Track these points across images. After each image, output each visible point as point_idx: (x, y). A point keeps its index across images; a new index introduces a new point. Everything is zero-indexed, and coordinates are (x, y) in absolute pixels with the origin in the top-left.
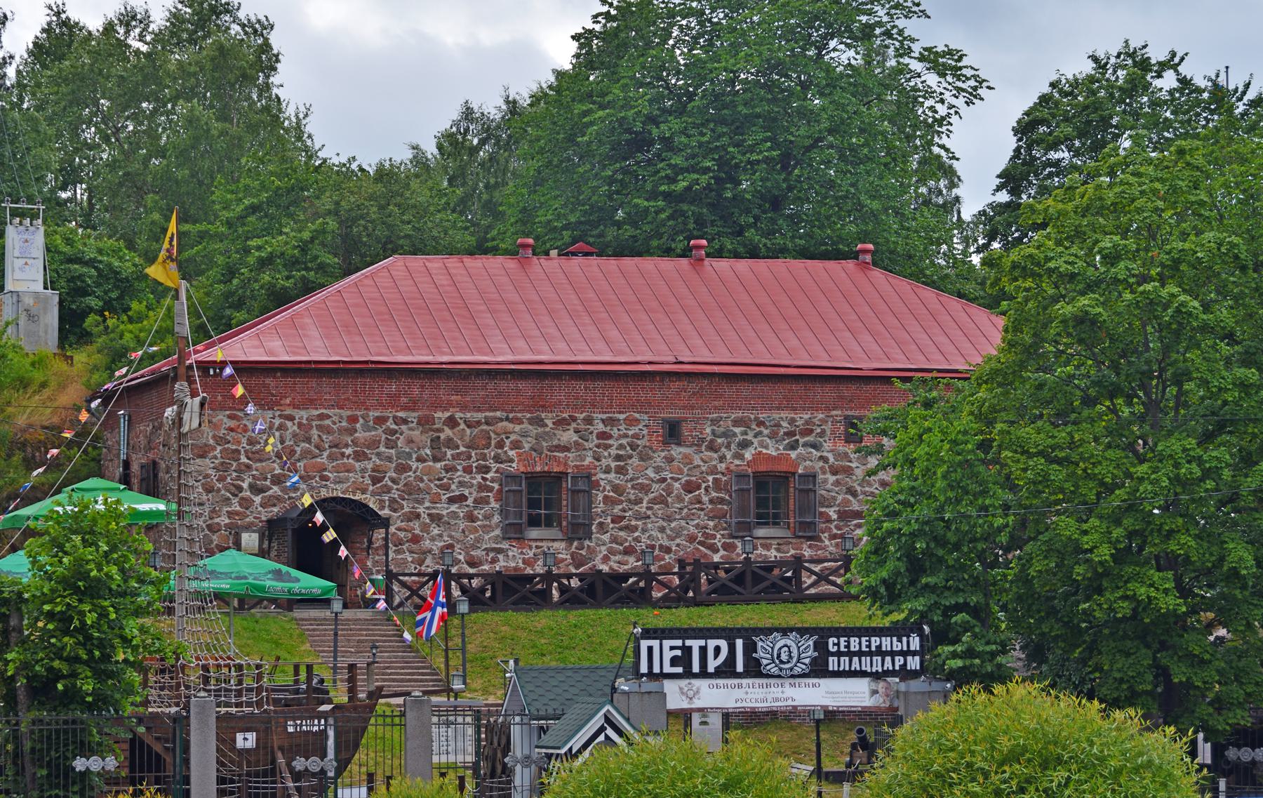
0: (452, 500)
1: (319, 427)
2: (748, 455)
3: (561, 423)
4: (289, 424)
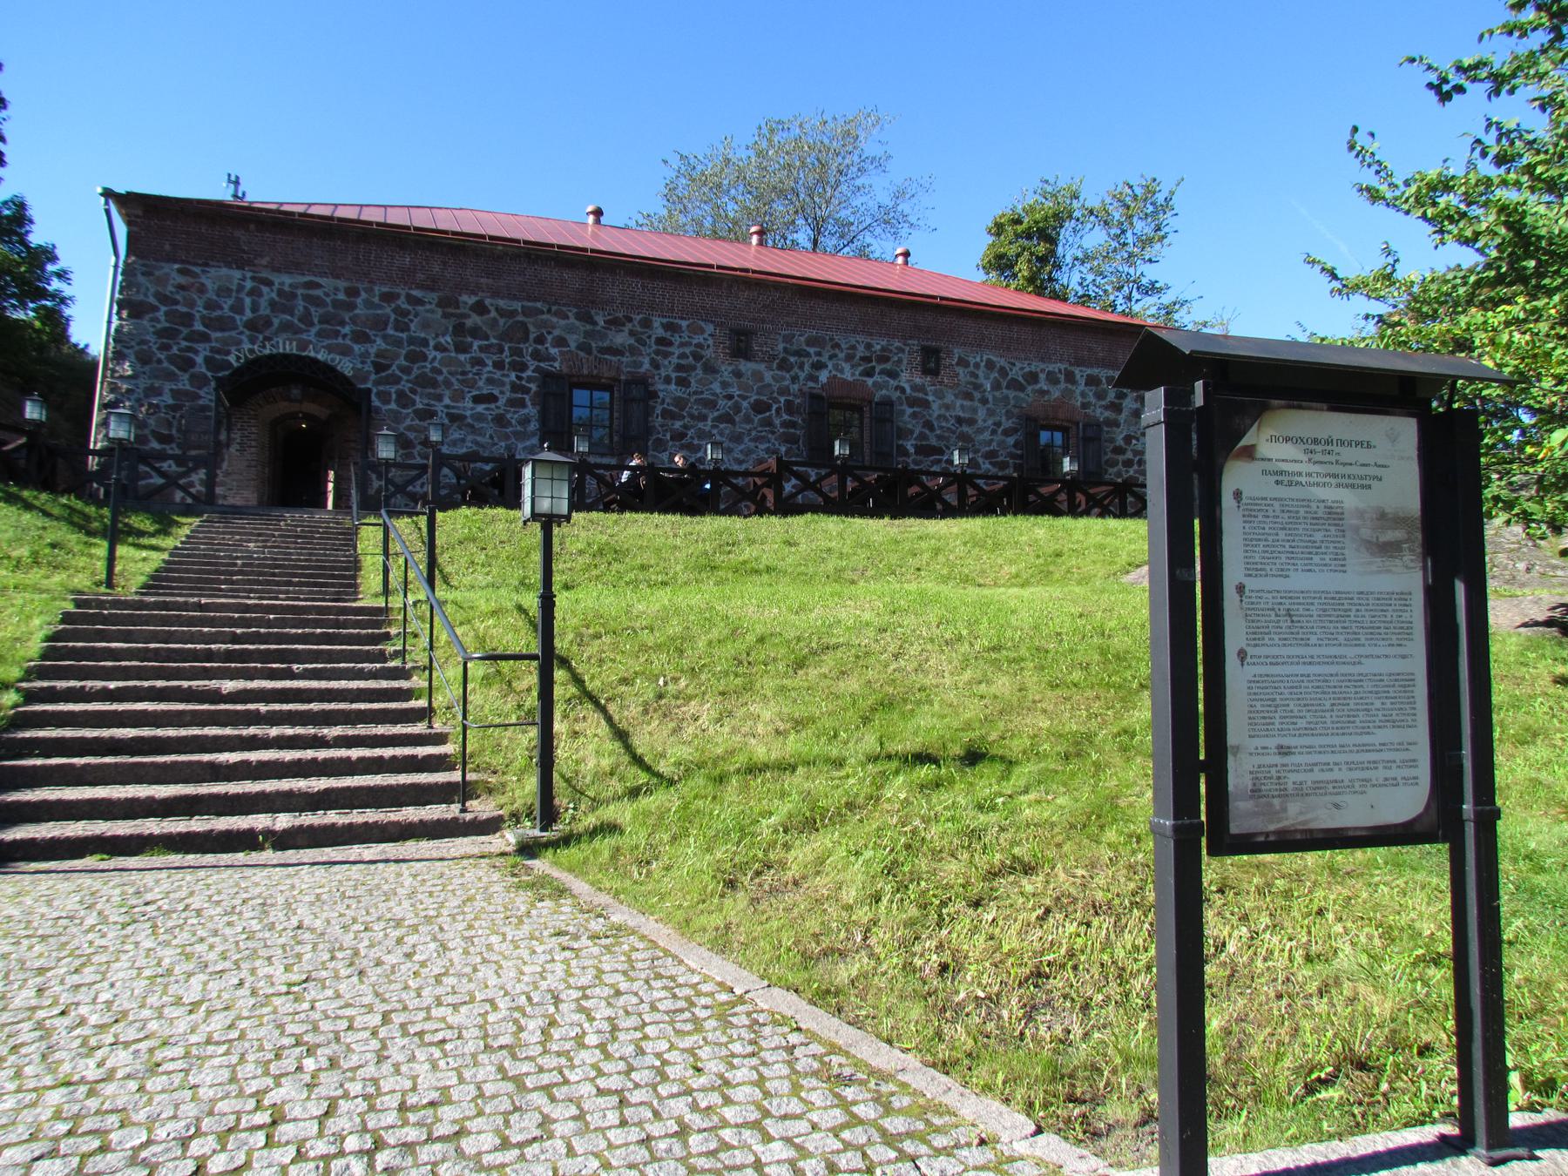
0: (478, 400)
1: (307, 298)
2: (823, 376)
3: (614, 323)
4: (265, 289)
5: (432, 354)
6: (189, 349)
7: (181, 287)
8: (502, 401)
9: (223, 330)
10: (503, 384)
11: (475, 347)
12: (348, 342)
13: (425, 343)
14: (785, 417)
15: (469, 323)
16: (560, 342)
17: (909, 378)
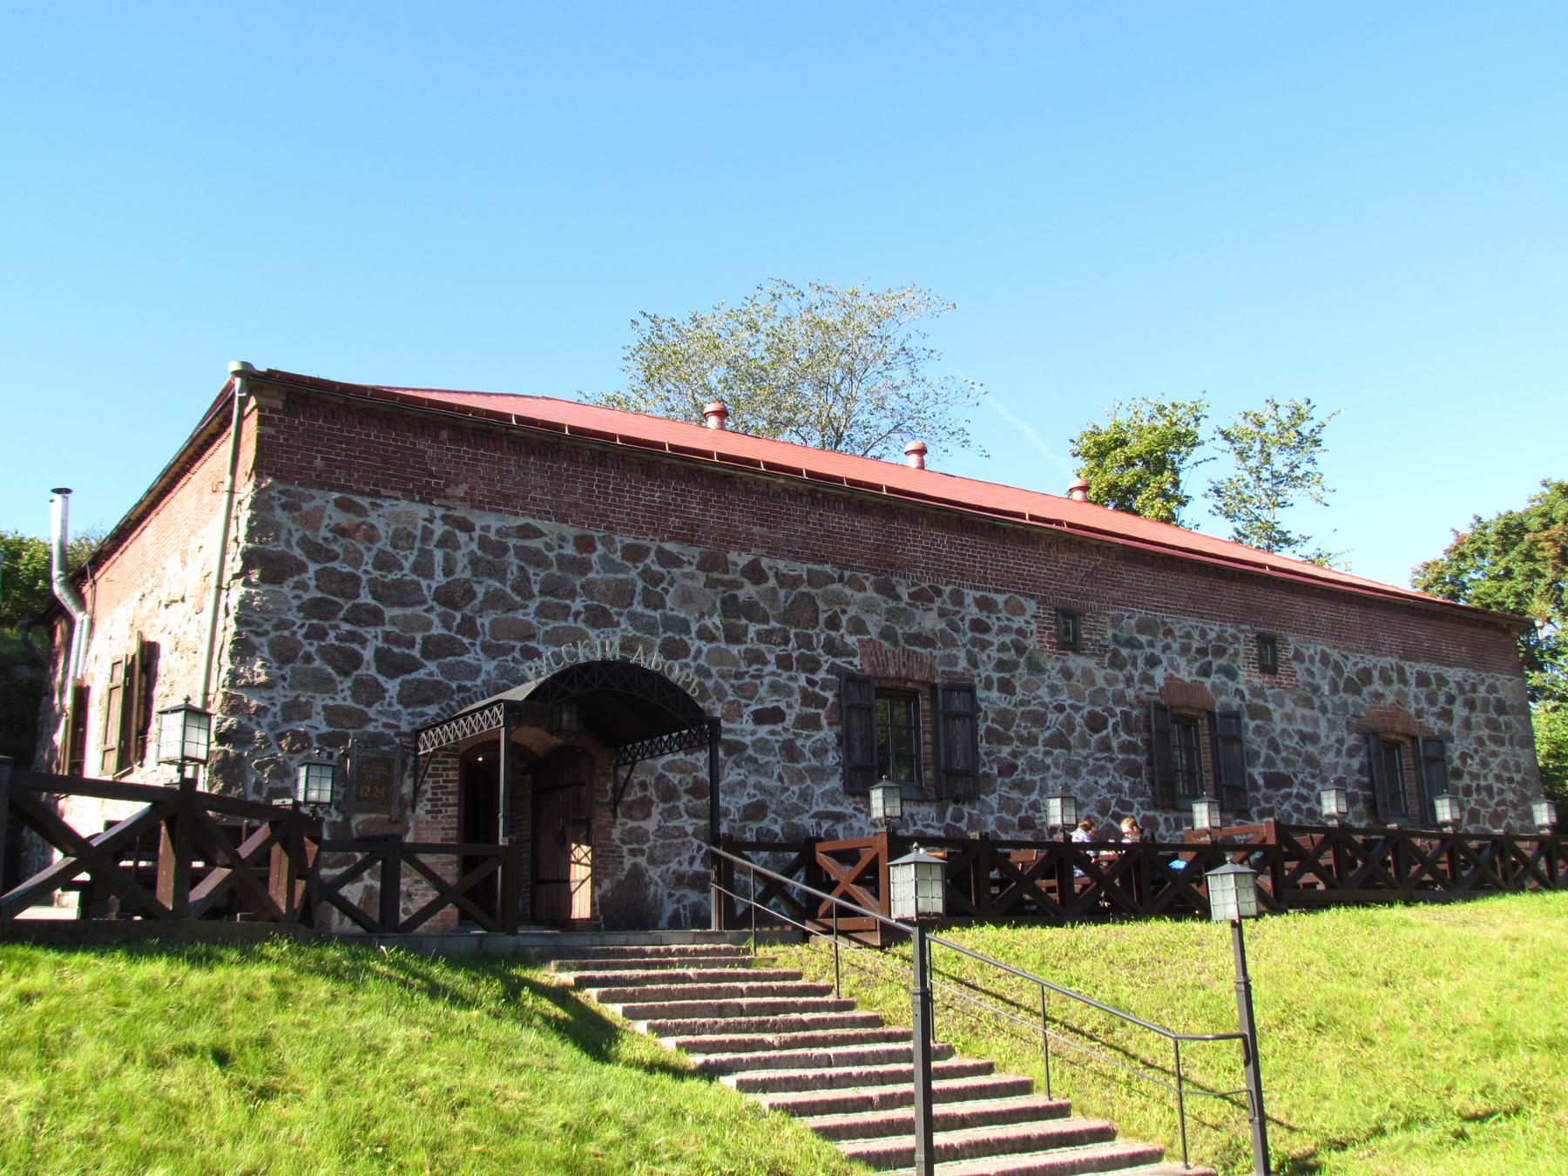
0: (761, 717)
1: (522, 553)
2: (1159, 675)
3: (919, 596)
4: (462, 537)
5: (695, 644)
6: (352, 637)
7: (341, 531)
8: (790, 720)
9: (404, 604)
10: (790, 693)
11: (751, 634)
12: (581, 625)
13: (684, 626)
14: (1124, 737)
15: (742, 595)
16: (858, 626)
17: (1249, 677)
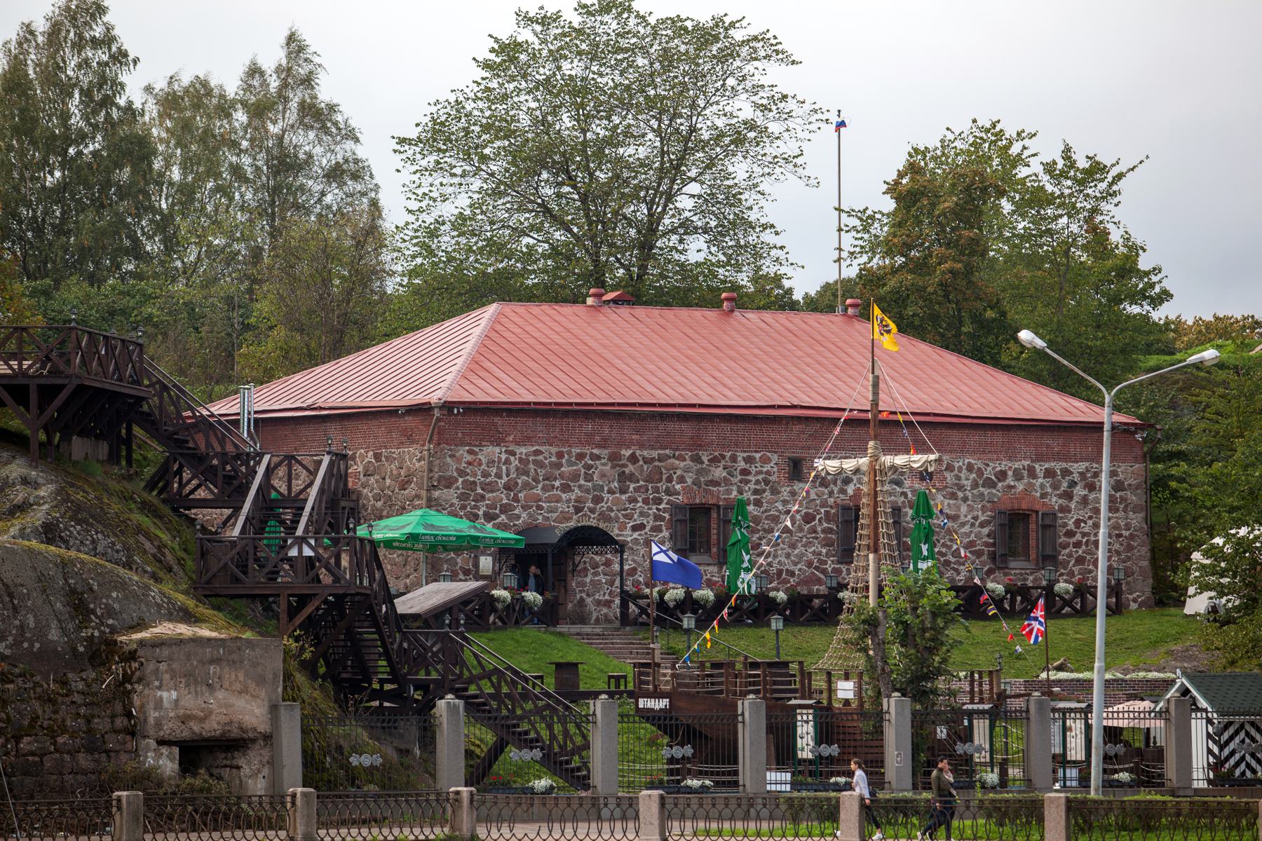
0: (634, 528)
1: (535, 462)
3: (714, 460)
4: (512, 458)
7: (469, 463)
13: (602, 487)
16: (682, 480)
